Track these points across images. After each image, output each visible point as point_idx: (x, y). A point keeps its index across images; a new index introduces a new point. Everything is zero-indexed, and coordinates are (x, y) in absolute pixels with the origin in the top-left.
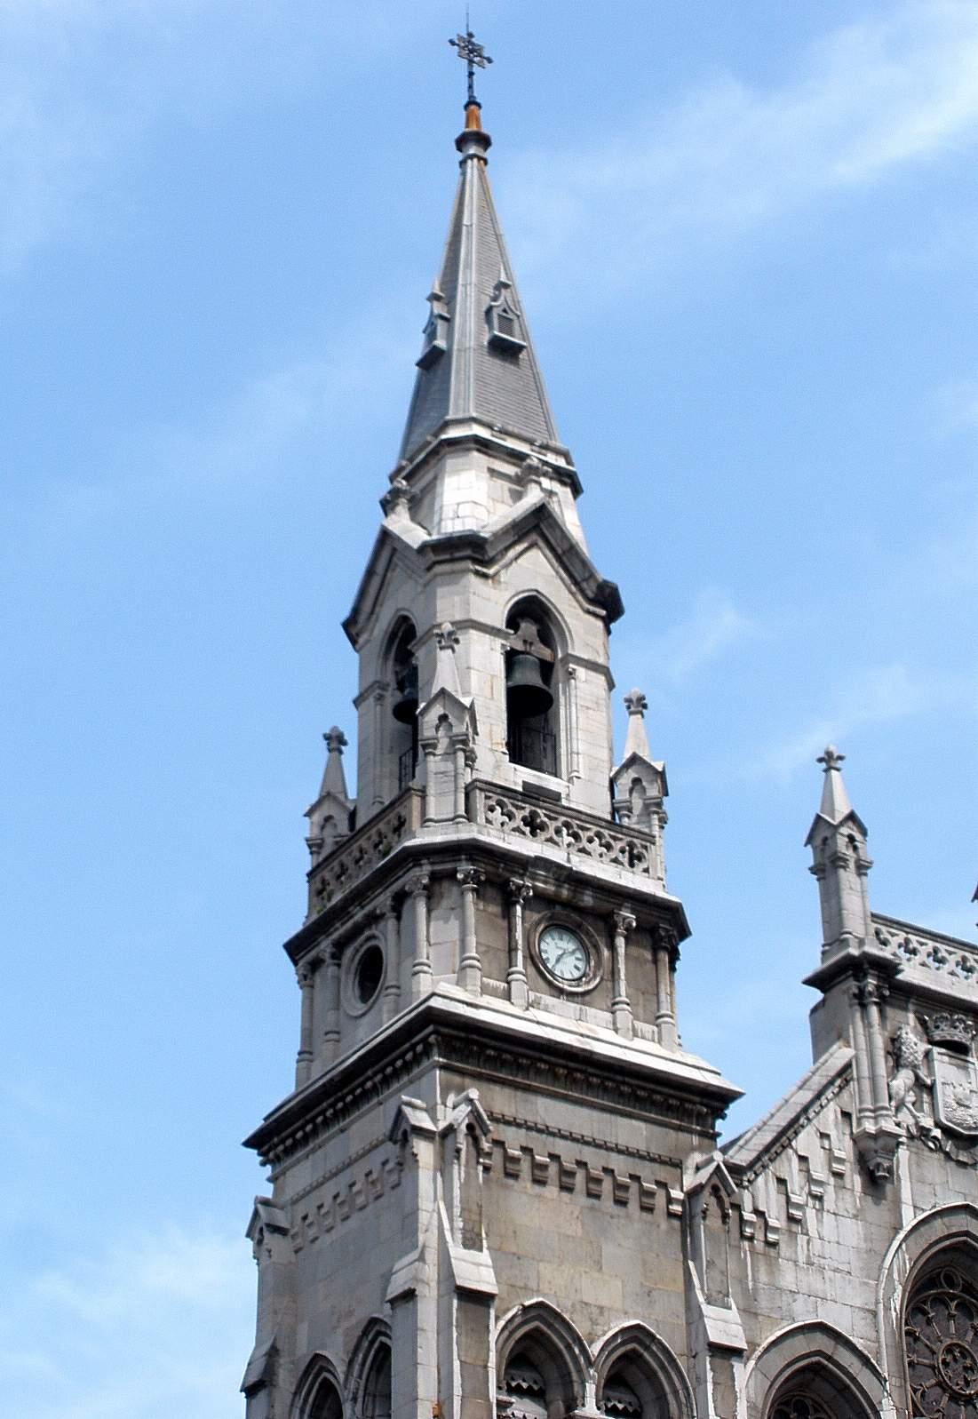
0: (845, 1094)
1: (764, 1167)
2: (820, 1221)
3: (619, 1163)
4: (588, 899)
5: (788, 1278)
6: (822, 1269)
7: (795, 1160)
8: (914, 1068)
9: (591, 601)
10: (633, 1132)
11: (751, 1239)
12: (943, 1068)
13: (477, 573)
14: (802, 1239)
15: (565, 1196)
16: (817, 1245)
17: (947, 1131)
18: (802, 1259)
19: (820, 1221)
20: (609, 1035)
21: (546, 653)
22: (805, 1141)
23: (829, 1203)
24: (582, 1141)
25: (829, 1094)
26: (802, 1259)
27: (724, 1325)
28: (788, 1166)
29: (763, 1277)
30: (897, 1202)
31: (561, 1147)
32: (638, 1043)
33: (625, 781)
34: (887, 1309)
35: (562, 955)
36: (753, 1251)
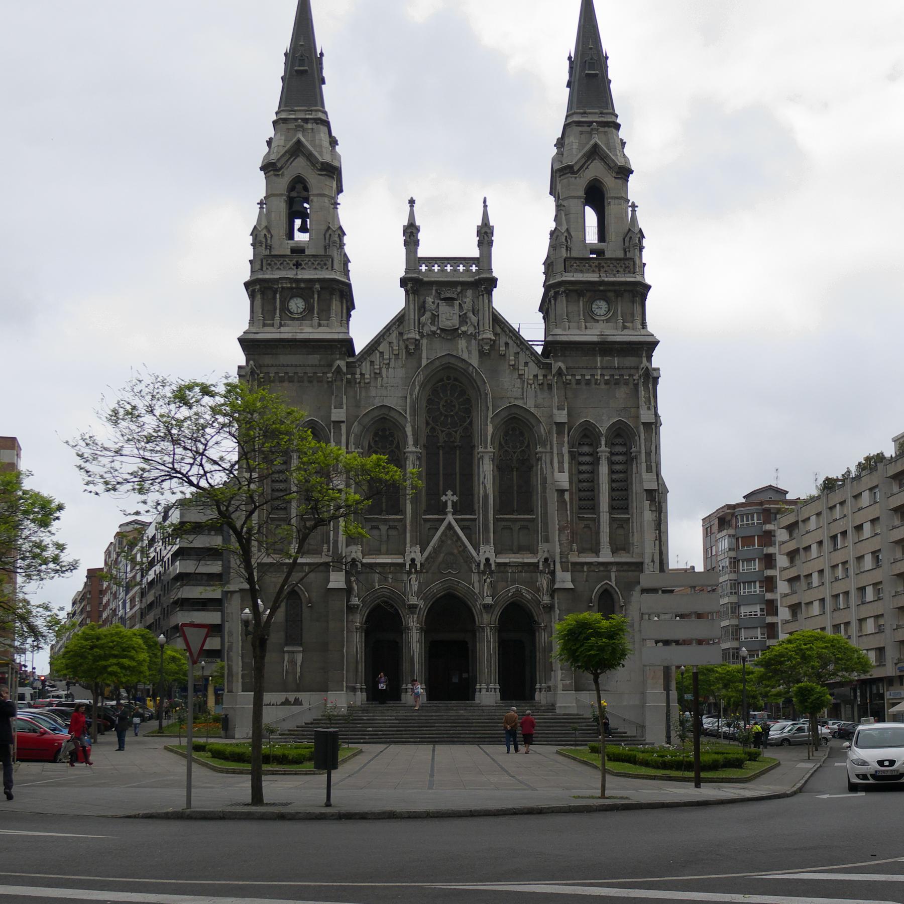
0: (401, 327)
1: (365, 359)
2: (387, 371)
3: (309, 370)
4: (303, 285)
5: (373, 392)
6: (386, 387)
7: (378, 355)
8: (430, 311)
9: (321, 170)
10: (314, 359)
11: (360, 383)
12: (444, 308)
13: (276, 175)
14: (379, 379)
15: (291, 384)
16: (385, 379)
17: (442, 330)
18: (379, 385)
19: (387, 371)
20: (310, 330)
21: (305, 194)
22: (383, 347)
23: (392, 365)
24: (296, 366)
25: (393, 328)
26: (379, 385)
27: (338, 414)
28: (376, 357)
29: (363, 394)
30: (420, 359)
31: (289, 369)
32: (321, 329)
33: (327, 236)
34: (411, 395)
35: (297, 305)
36: (360, 387)
